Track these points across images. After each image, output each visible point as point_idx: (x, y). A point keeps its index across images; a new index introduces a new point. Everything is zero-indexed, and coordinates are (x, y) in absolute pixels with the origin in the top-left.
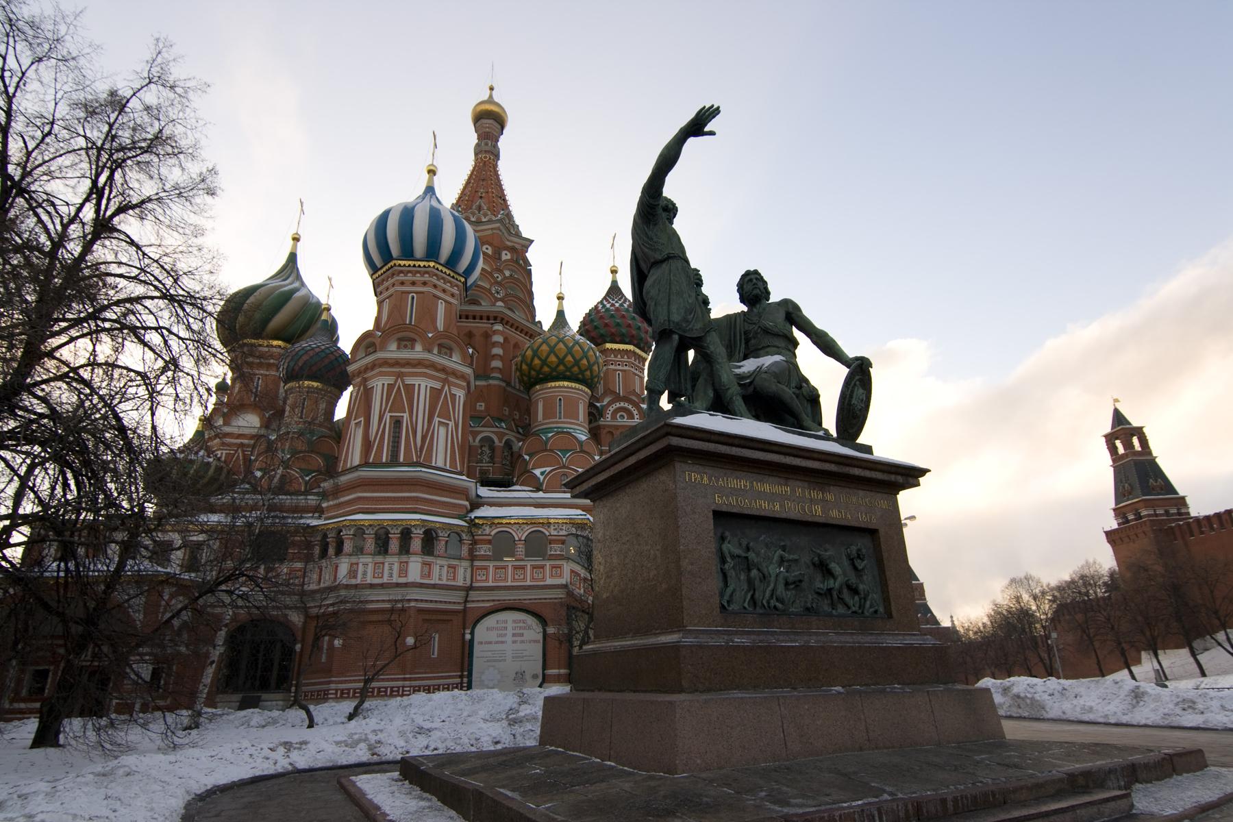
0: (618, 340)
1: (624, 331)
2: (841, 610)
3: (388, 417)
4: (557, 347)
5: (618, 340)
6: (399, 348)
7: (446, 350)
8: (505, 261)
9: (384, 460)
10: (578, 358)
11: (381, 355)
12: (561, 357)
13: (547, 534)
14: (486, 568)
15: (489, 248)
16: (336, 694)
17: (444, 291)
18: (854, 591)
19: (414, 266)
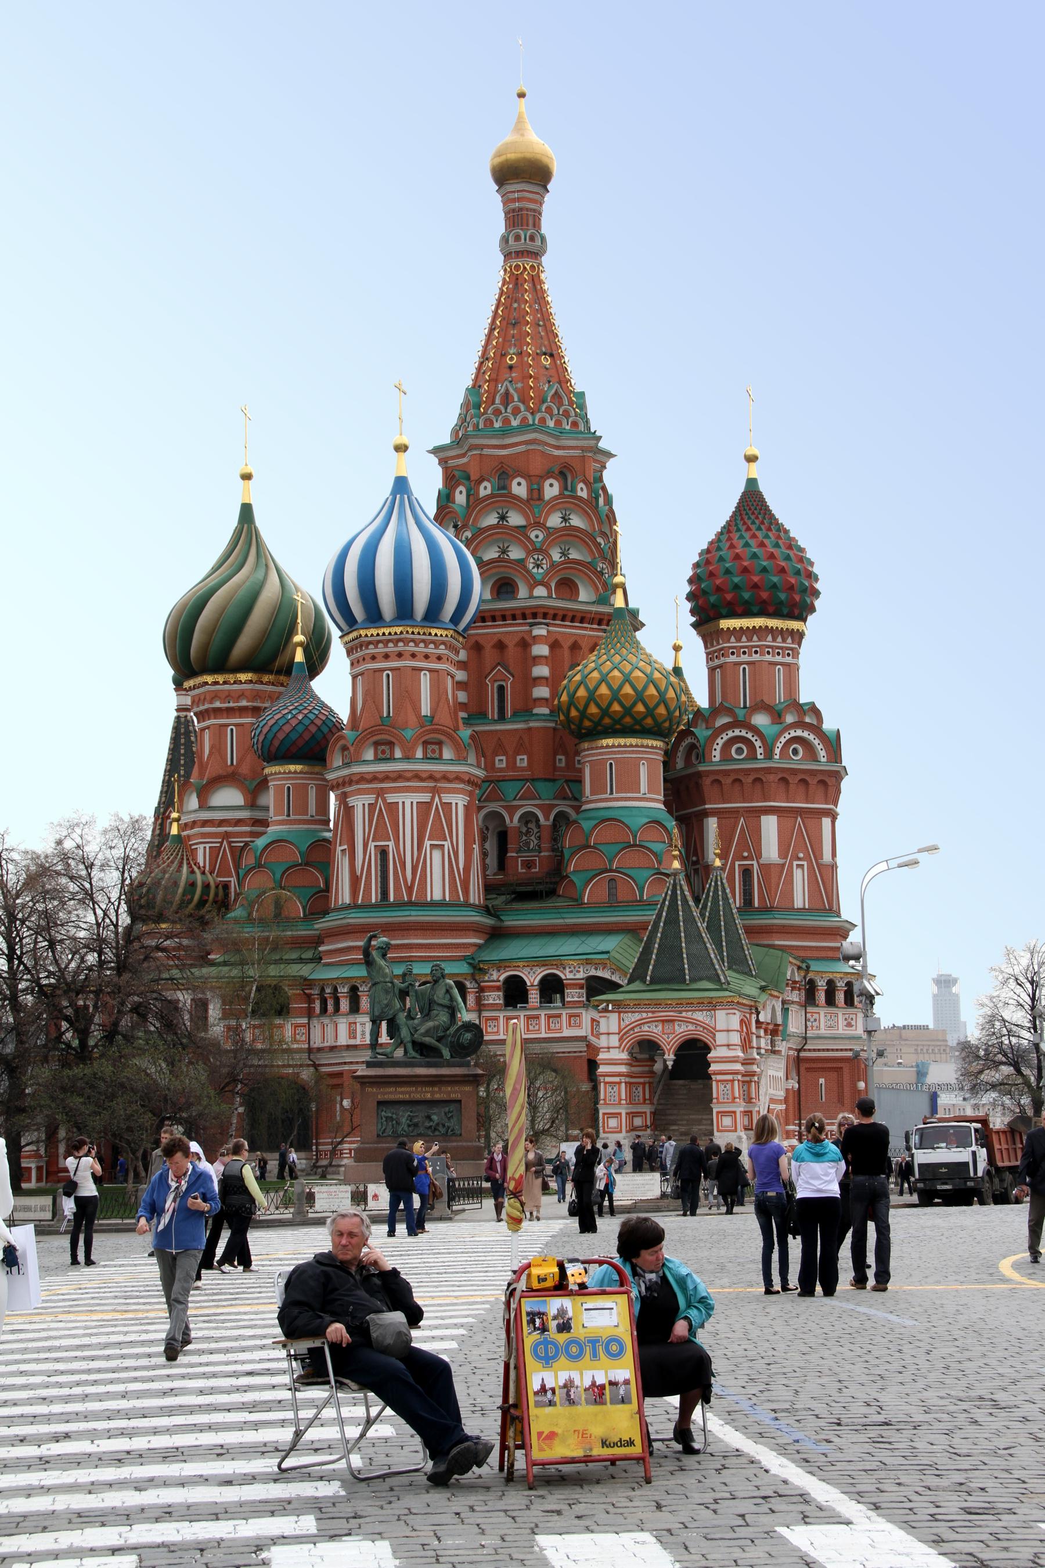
0: (739, 611)
1: (746, 595)
2: (437, 1133)
3: (373, 848)
4: (597, 693)
5: (739, 611)
7: (433, 746)
8: (549, 502)
9: (373, 901)
10: (628, 705)
12: (604, 707)
13: (563, 977)
14: (496, 1019)
15: (523, 482)
16: (350, 1153)
17: (427, 657)
18: (444, 1126)
19: (384, 634)
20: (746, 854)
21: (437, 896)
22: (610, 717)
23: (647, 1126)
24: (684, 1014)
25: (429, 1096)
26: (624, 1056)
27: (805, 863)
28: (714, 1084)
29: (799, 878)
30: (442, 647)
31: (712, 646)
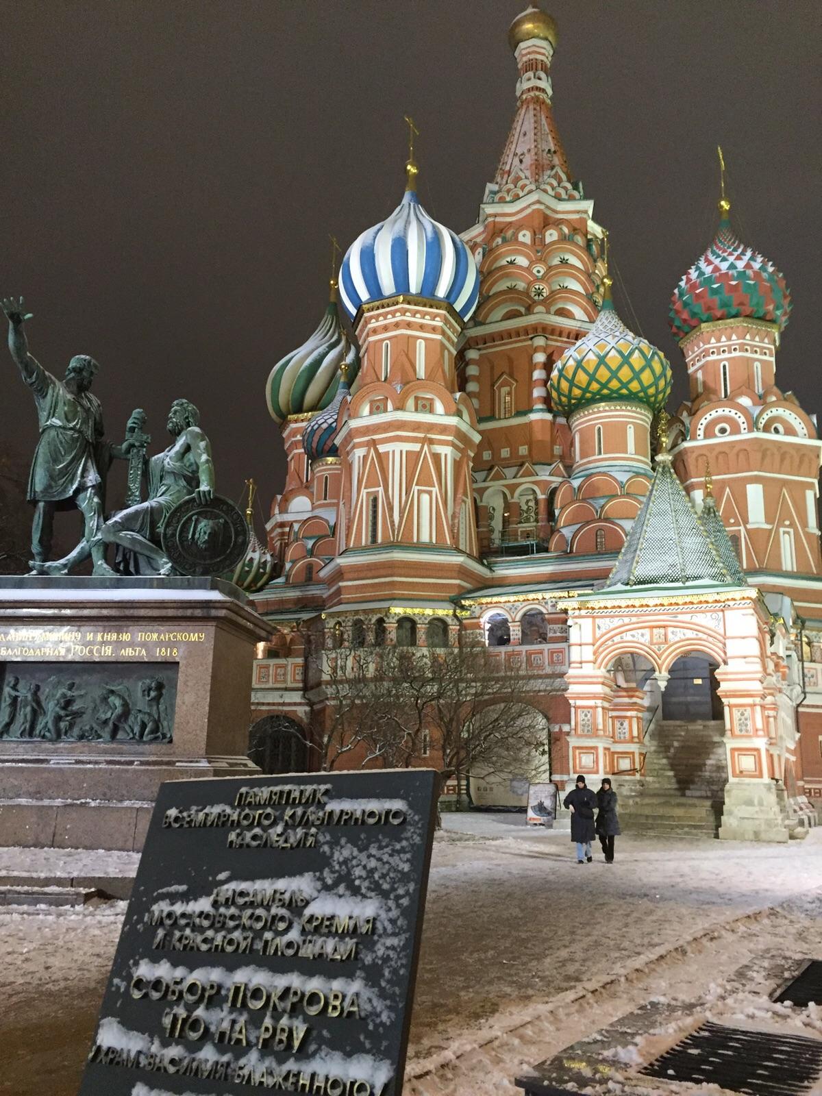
0: (719, 314)
6: (371, 413)
7: (424, 402)
11: (354, 424)
12: (591, 372)
17: (422, 327)
20: (732, 521)
21: (425, 538)
22: (598, 382)
23: (635, 769)
24: (680, 617)
25: (107, 653)
26: (602, 672)
27: (791, 531)
28: (726, 710)
29: (787, 544)
30: (438, 319)
31: (693, 352)
